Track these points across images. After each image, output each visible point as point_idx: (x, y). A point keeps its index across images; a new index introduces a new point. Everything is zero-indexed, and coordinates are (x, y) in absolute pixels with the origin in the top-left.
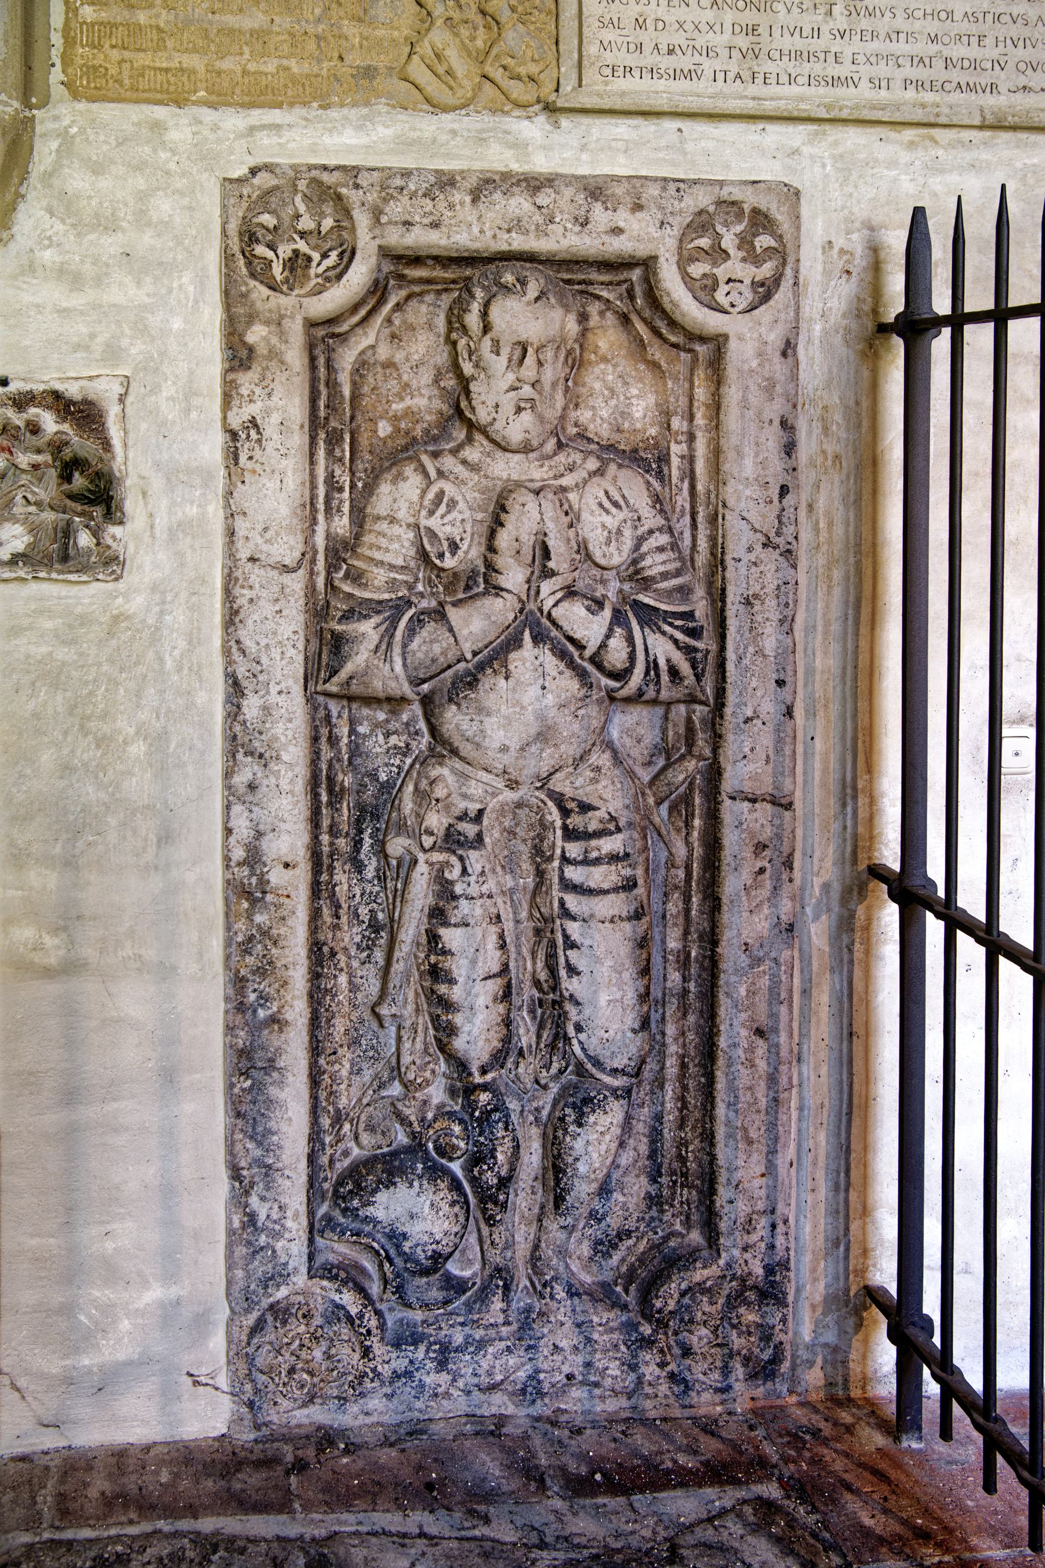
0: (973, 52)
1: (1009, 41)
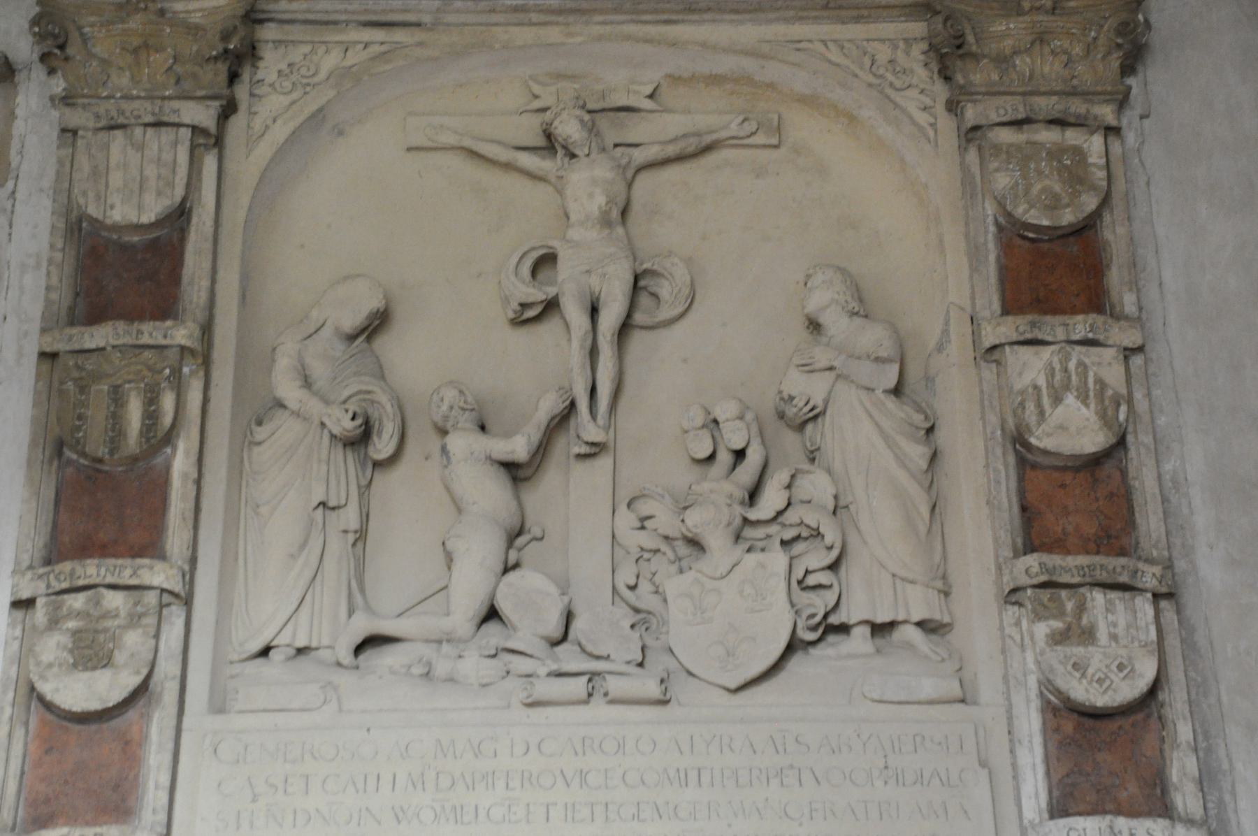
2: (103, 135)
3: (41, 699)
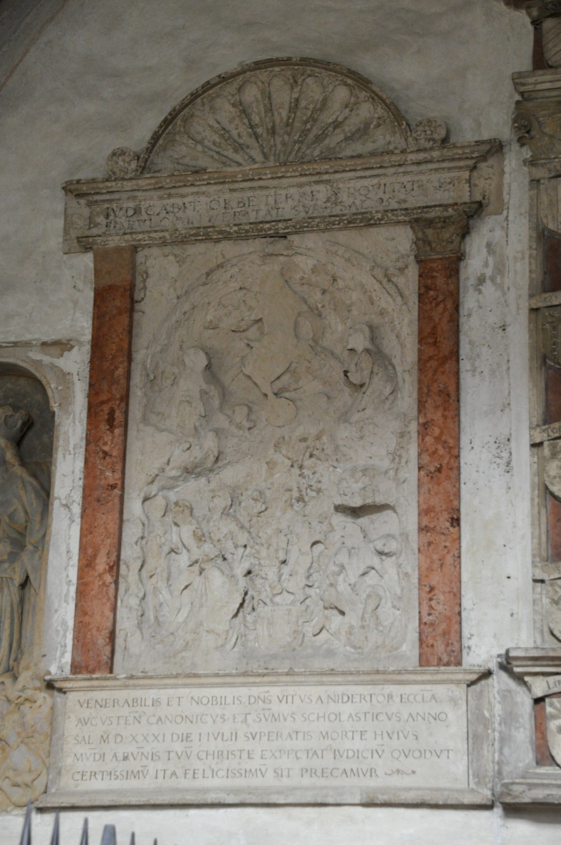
0: (358, 744)
1: (385, 735)
2: (553, 181)
3: (552, 494)
